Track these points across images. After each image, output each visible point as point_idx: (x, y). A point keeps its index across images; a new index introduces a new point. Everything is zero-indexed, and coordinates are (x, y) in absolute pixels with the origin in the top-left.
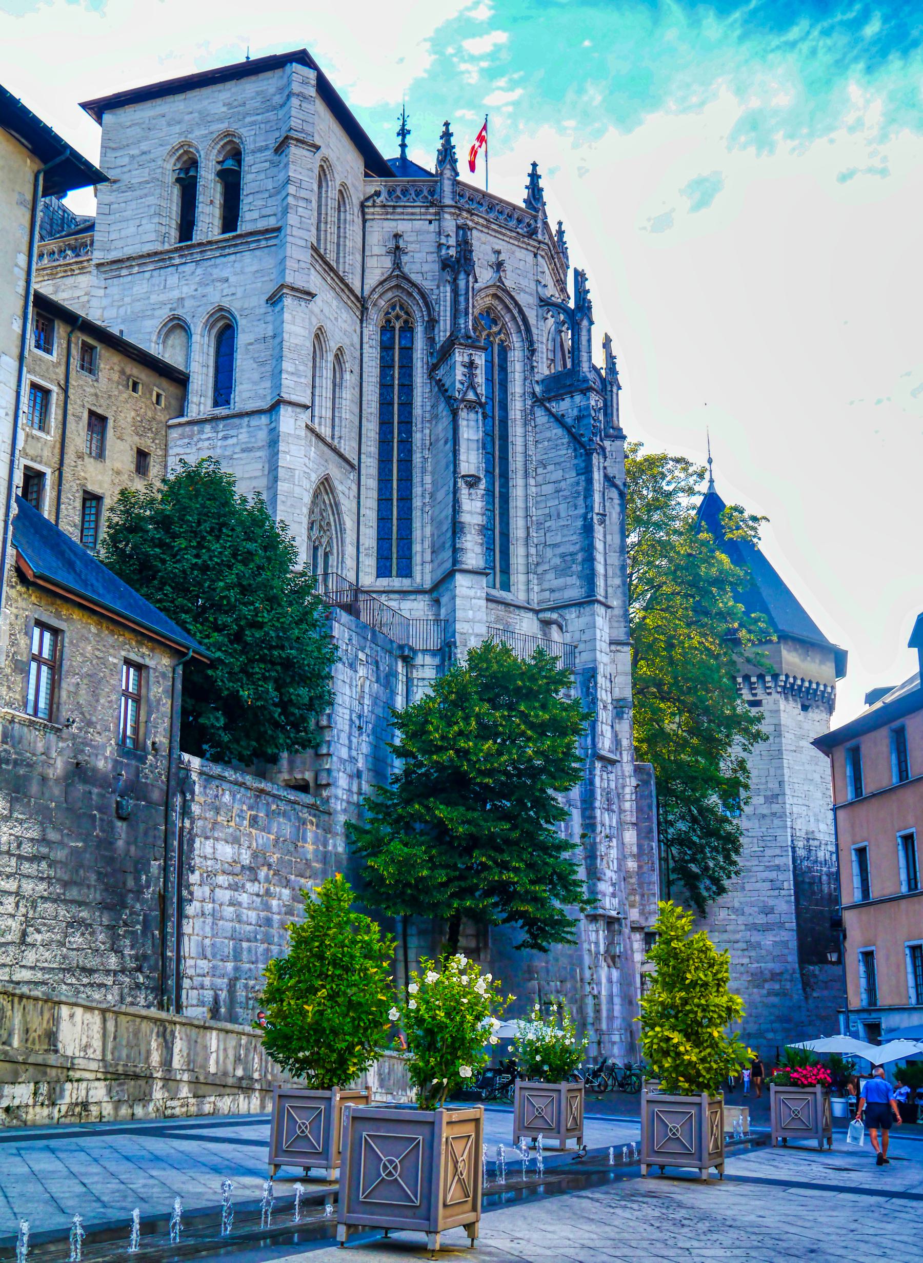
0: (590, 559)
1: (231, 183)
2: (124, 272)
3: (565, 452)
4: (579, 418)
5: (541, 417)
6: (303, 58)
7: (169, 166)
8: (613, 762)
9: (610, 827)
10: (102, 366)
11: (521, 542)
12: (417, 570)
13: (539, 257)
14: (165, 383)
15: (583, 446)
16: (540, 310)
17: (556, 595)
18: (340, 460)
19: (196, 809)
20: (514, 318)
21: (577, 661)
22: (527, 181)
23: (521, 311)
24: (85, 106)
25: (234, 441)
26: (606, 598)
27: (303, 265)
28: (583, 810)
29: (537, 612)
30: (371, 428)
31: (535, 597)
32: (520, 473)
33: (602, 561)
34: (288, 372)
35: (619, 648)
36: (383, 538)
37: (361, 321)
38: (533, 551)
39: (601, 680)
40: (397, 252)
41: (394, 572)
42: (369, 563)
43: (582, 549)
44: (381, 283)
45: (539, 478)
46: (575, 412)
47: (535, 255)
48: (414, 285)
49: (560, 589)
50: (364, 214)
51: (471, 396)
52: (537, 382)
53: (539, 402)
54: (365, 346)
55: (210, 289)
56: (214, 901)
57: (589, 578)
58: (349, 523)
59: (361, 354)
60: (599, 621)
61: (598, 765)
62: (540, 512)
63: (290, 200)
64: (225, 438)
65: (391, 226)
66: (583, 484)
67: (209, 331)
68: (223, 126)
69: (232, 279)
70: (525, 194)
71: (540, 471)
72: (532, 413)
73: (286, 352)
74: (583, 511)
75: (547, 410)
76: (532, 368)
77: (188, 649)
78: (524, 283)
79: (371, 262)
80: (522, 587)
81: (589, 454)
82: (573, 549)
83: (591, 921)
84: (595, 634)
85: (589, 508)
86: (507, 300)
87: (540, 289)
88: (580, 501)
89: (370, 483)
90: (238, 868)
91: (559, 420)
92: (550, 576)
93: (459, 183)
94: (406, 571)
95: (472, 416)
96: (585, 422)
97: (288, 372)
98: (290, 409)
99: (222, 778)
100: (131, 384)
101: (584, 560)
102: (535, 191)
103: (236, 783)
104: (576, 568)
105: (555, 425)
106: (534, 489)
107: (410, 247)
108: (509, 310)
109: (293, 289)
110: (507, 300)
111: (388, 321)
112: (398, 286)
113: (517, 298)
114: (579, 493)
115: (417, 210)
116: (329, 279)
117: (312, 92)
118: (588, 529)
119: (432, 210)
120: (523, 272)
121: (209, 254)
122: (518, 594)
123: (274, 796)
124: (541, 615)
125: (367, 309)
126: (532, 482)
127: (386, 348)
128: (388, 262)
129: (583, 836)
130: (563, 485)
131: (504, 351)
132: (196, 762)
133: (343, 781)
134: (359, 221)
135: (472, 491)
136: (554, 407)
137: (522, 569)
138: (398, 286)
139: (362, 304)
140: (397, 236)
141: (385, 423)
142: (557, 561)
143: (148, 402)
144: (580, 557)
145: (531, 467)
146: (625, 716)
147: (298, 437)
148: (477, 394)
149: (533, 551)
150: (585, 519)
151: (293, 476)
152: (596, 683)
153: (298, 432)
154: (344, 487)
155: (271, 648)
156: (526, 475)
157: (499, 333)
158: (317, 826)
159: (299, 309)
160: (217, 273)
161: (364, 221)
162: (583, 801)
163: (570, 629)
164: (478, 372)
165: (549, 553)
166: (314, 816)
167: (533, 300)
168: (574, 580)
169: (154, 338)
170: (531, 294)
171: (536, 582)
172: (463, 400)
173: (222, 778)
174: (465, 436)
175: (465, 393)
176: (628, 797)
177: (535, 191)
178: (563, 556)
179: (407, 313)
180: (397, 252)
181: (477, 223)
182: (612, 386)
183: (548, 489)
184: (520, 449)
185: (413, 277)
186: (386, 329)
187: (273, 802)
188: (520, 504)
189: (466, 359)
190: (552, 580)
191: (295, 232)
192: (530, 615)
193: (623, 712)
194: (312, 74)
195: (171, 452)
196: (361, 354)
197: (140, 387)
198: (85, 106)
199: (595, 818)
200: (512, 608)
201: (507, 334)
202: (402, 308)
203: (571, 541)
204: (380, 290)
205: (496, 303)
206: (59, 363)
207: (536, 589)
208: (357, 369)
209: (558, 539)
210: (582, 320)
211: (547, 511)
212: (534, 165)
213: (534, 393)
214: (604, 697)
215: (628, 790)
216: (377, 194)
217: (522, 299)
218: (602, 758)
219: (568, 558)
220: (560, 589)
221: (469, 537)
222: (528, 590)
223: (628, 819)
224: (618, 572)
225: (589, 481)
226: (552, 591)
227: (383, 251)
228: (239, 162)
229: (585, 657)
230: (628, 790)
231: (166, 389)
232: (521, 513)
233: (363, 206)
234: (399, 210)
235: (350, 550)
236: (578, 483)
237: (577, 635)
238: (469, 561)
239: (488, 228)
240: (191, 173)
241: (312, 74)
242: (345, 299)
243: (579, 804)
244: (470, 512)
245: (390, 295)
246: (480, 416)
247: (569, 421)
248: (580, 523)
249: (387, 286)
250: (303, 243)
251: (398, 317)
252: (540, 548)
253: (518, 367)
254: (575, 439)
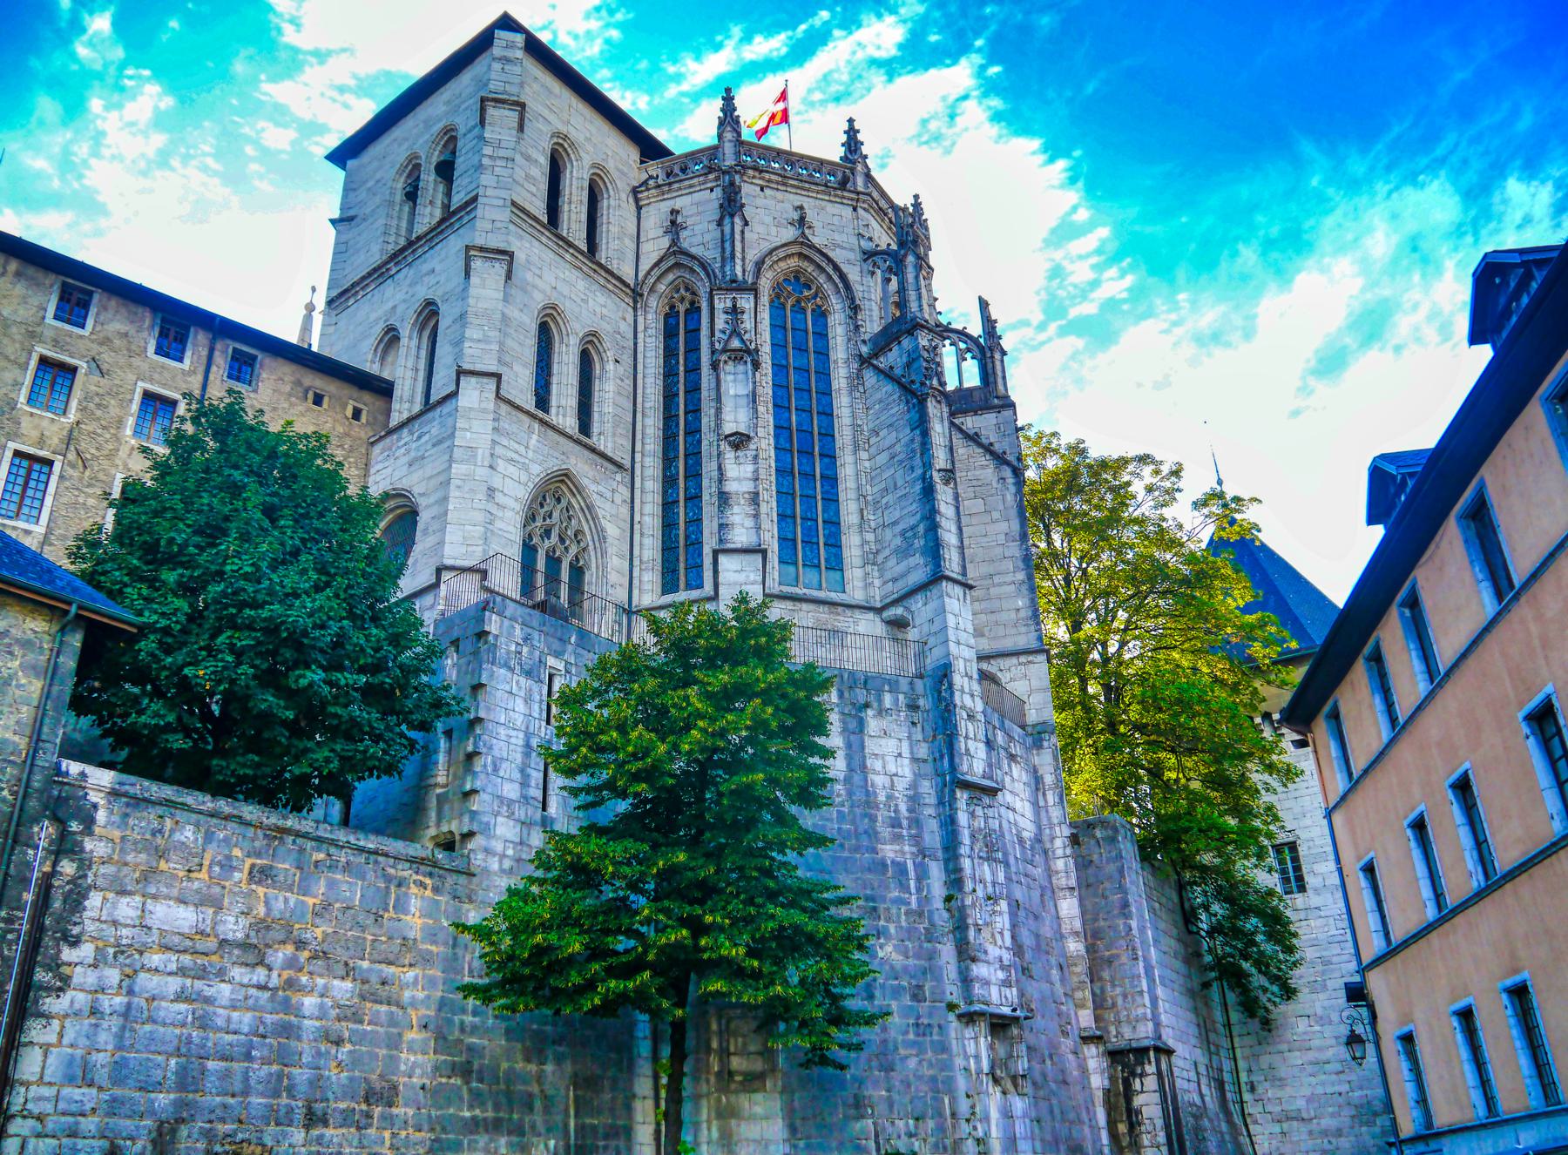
0: (933, 528)
2: (351, 301)
3: (898, 408)
4: (908, 365)
5: (870, 377)
7: (400, 185)
8: (992, 792)
9: (994, 884)
10: (264, 375)
13: (860, 211)
14: (367, 397)
15: (913, 393)
16: (865, 266)
17: (900, 584)
18: (592, 456)
19: (94, 847)
20: (830, 278)
21: (928, 661)
22: (844, 138)
23: (836, 267)
25: (426, 438)
26: (964, 574)
27: (498, 225)
28: (946, 861)
29: (878, 611)
30: (652, 425)
32: (849, 449)
33: (954, 528)
34: (472, 340)
35: (1031, 658)
36: (669, 549)
37: (635, 309)
38: (870, 537)
39: (958, 680)
40: (674, 226)
41: (682, 584)
43: (923, 518)
44: (656, 265)
45: (873, 450)
46: (905, 359)
47: (855, 209)
48: (693, 257)
49: (903, 575)
50: (637, 200)
51: (736, 344)
52: (864, 342)
53: (864, 361)
54: (640, 336)
55: (418, 287)
56: (130, 992)
57: (934, 550)
58: (614, 532)
59: (635, 344)
60: (952, 604)
61: (962, 796)
62: (876, 489)
63: (485, 161)
64: (419, 438)
65: (666, 207)
66: (918, 439)
67: (421, 331)
68: (440, 125)
69: (438, 269)
70: (841, 151)
71: (873, 441)
72: (859, 376)
73: (471, 318)
74: (919, 471)
75: (876, 367)
76: (857, 327)
77: (70, 604)
79: (645, 248)
81: (922, 402)
82: (913, 521)
83: (967, 1024)
84: (945, 621)
85: (928, 465)
86: (817, 258)
87: (863, 243)
88: (917, 461)
90: (212, 944)
91: (887, 374)
92: (892, 562)
93: (742, 143)
95: (741, 368)
96: (915, 365)
97: (472, 340)
98: (473, 380)
99: (185, 807)
100: (311, 396)
101: (927, 531)
102: (852, 142)
103: (213, 814)
104: (919, 543)
105: (886, 381)
106: (867, 464)
108: (830, 278)
109: (481, 249)
110: (817, 258)
111: (672, 307)
112: (677, 265)
113: (831, 254)
114: (913, 451)
115: (695, 181)
116: (568, 256)
118: (928, 491)
119: (711, 176)
120: (837, 228)
121: (420, 251)
122: (856, 594)
123: (318, 839)
124: (885, 614)
125: (641, 295)
127: (670, 334)
129: (948, 899)
130: (898, 448)
131: (822, 315)
132: (103, 778)
133: (505, 829)
134: (633, 207)
135: (739, 453)
136: (882, 362)
137: (857, 561)
138: (677, 265)
139: (636, 295)
140: (675, 212)
141: (669, 418)
142: (898, 541)
143: (339, 417)
144: (921, 529)
146: (1045, 744)
147: (484, 411)
148: (743, 341)
150: (924, 479)
151: (475, 456)
152: (951, 685)
153: (484, 405)
155: (243, 605)
157: (815, 297)
158: (436, 890)
159: (492, 271)
160: (426, 267)
161: (639, 208)
162: (946, 849)
163: (917, 622)
164: (745, 316)
165: (888, 533)
166: (431, 875)
167: (856, 256)
168: (918, 559)
169: (370, 357)
170: (852, 250)
171: (876, 574)
172: (724, 351)
173: (185, 807)
174: (732, 392)
175: (727, 342)
176: (1059, 852)
177: (852, 142)
178: (903, 533)
179: (694, 293)
181: (769, 181)
182: (992, 351)
183: (883, 458)
184: (847, 421)
185: (693, 251)
186: (671, 316)
187: (318, 850)
188: (851, 484)
189: (729, 304)
190: (895, 567)
191: (489, 192)
193: (1042, 740)
194: (519, 39)
195: (373, 471)
196: (635, 344)
197: (326, 400)
199: (961, 870)
200: (840, 609)
201: (825, 298)
202: (687, 289)
203: (908, 513)
204: (656, 273)
205: (805, 265)
206: (193, 372)
207: (877, 582)
208: (627, 359)
209: (897, 514)
210: (905, 256)
211: (883, 485)
212: (851, 121)
214: (968, 701)
215: (1058, 843)
218: (966, 785)
219: (909, 534)
220: (903, 575)
221: (736, 509)
222: (867, 586)
223: (1063, 882)
224: (1021, 565)
225: (925, 434)
226: (895, 580)
227: (660, 232)
229: (937, 653)
230: (1058, 843)
231: (368, 402)
232: (852, 495)
233: (635, 191)
234: (676, 186)
236: (912, 440)
237: (926, 629)
238: (736, 539)
239: (784, 184)
242: (602, 281)
243: (940, 854)
244: (738, 479)
245: (671, 277)
246: (749, 365)
247: (898, 372)
248: (918, 487)
249: (664, 266)
250: (501, 202)
251: (682, 299)
252: (879, 531)
253: (840, 330)
254: (905, 388)
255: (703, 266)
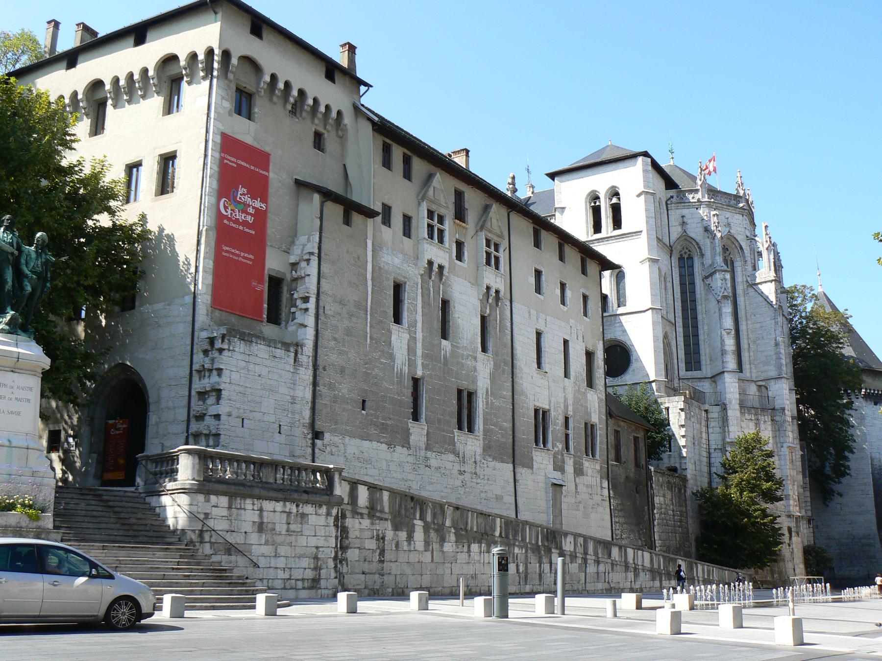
1: (616, 210)
6: (646, 154)
11: (746, 351)
12: (703, 367)
24: (547, 175)
31: (754, 375)
32: (744, 318)
40: (683, 224)
42: (682, 365)
78: (739, 229)
80: (748, 371)
89: (680, 330)
94: (699, 368)
104: (773, 362)
107: (689, 221)
117: (650, 168)
126: (749, 322)
128: (679, 229)
137: (747, 362)
140: (683, 217)
145: (748, 316)
149: (752, 354)
154: (672, 335)
156: (747, 320)
168: (772, 367)
180: (683, 224)
186: (681, 259)
192: (753, 384)
194: (649, 160)
198: (547, 175)
213: (747, 281)
216: (672, 197)
217: (739, 238)
228: (619, 199)
232: (745, 337)
233: (667, 204)
235: (675, 361)
240: (598, 204)
241: (649, 160)
255: (697, 244)
